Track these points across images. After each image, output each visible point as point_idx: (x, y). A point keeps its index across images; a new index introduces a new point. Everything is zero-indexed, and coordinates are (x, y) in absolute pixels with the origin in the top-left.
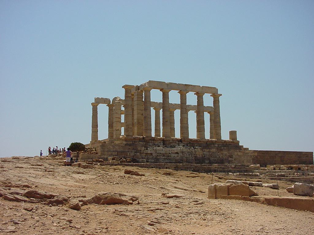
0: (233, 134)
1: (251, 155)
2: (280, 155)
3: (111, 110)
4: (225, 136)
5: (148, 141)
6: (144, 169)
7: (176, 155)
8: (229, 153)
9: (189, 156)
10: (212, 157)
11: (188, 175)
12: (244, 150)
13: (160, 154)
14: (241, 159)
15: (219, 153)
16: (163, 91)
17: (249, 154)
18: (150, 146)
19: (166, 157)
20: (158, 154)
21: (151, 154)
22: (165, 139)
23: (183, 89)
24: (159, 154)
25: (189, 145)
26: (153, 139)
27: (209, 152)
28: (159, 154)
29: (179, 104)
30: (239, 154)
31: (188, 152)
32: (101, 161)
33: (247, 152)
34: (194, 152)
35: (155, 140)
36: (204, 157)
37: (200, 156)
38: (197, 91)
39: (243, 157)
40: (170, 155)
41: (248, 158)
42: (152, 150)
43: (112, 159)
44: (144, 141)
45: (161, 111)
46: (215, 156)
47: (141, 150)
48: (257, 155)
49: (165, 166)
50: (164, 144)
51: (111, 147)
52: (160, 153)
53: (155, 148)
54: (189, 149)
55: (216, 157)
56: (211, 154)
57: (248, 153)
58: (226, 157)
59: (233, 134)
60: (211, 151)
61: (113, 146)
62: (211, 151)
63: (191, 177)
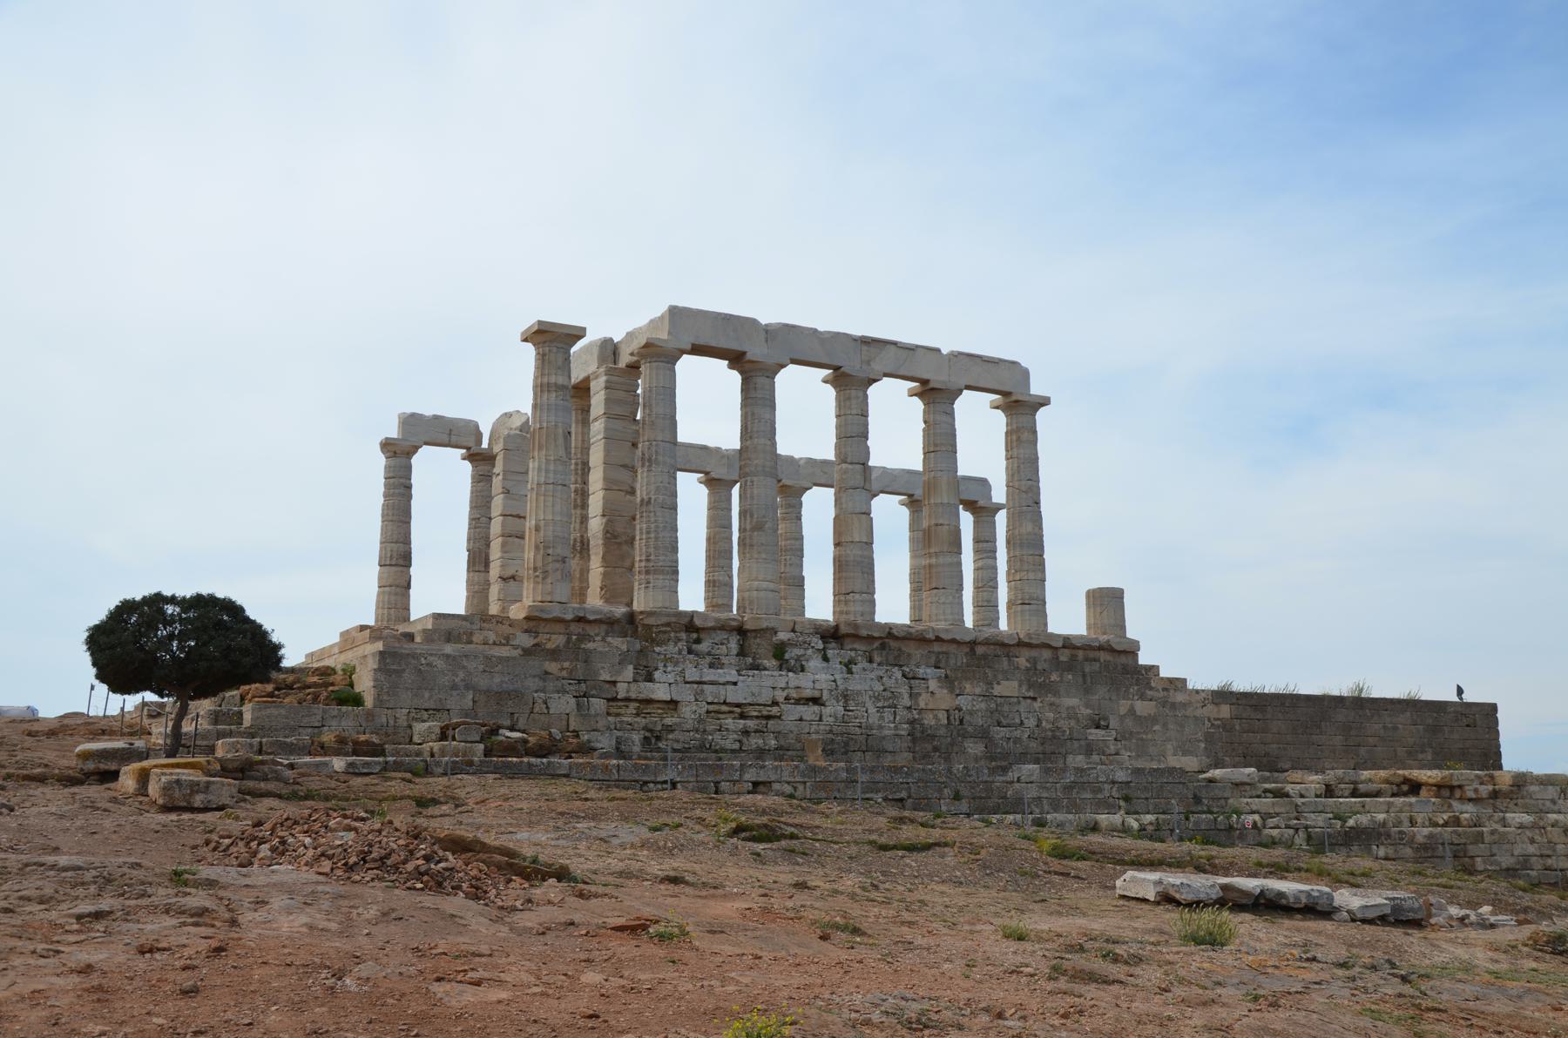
0: (1107, 602)
3: (482, 480)
4: (1067, 618)
5: (656, 634)
6: (613, 799)
7: (809, 711)
8: (1087, 706)
9: (882, 718)
10: (999, 724)
11: (883, 840)
12: (1165, 689)
15: (1037, 705)
16: (747, 366)
18: (666, 660)
19: (751, 724)
20: (711, 708)
21: (673, 704)
22: (747, 627)
23: (853, 366)
24: (715, 707)
25: (877, 659)
26: (685, 620)
27: (987, 696)
28: (715, 707)
29: (825, 462)
30: (1143, 708)
31: (877, 698)
32: (367, 742)
33: (1180, 698)
34: (906, 696)
35: (697, 630)
36: (961, 721)
37: (935, 717)
38: (925, 376)
39: (1156, 728)
40: (775, 710)
42: (676, 682)
43: (438, 731)
44: (635, 634)
45: (736, 491)
47: (614, 683)
49: (747, 777)
50: (742, 653)
51: (440, 664)
52: (725, 703)
53: (692, 674)
55: (1022, 723)
56: (993, 705)
57: (1184, 705)
58: (1073, 723)
59: (1107, 602)
60: (997, 690)
61: (448, 656)
62: (997, 690)
63: (900, 853)
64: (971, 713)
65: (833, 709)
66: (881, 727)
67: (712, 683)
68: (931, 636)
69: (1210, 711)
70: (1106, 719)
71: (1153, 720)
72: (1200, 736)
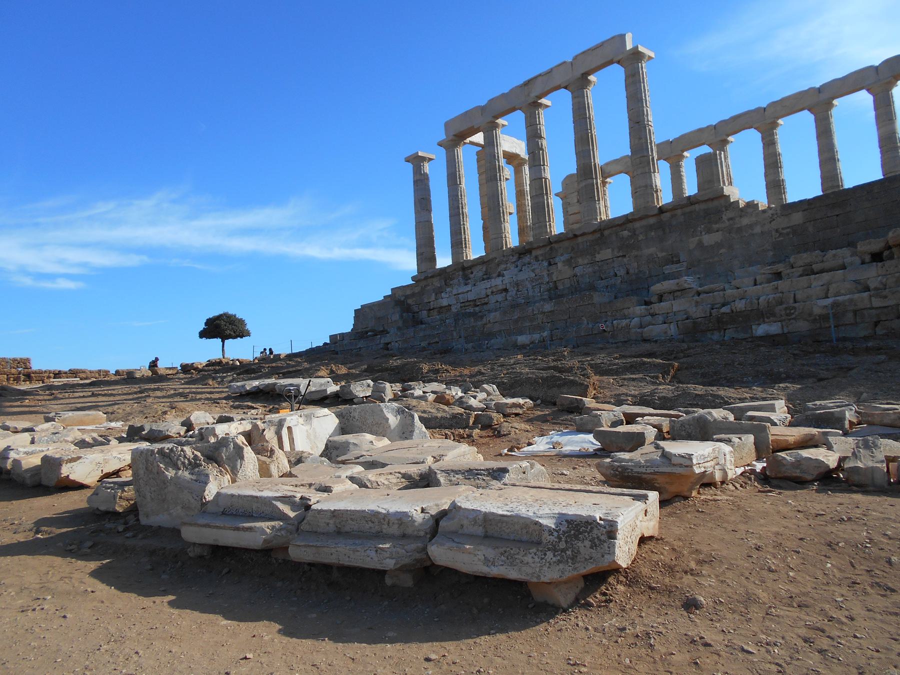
14: (716, 259)
15: (625, 260)
17: (758, 230)
19: (477, 309)
25: (540, 258)
27: (592, 263)
33: (745, 221)
34: (546, 276)
39: (722, 251)
46: (612, 274)
54: (533, 271)
55: (616, 275)
56: (597, 268)
57: (751, 226)
60: (598, 257)
62: (598, 257)
64: (582, 276)
65: (512, 292)
66: (534, 297)
71: (719, 245)
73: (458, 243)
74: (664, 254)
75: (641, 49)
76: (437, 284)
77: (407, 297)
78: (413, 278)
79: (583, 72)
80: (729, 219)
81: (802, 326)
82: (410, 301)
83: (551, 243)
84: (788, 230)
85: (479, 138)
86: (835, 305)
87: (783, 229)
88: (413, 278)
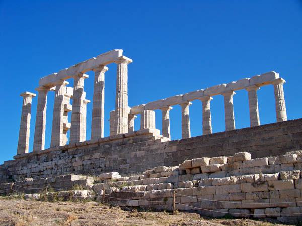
1: (162, 152)
2: (234, 140)
8: (120, 157)
13: (35, 174)
14: (141, 164)
17: (159, 152)
26: (36, 153)
27: (91, 159)
33: (155, 147)
39: (144, 160)
41: (156, 159)
48: (176, 150)
54: (65, 160)
55: (100, 167)
57: (156, 150)
60: (94, 157)
62: (94, 157)
64: (86, 165)
67: (34, 168)
68: (85, 144)
69: (168, 150)
70: (125, 160)
71: (143, 157)
72: (162, 161)
73: (37, 140)
74: (121, 159)
75: (124, 57)
76: (24, 161)
77: (9, 167)
78: (14, 157)
79: (101, 64)
80: (149, 145)
81: (146, 202)
82: (9, 169)
83: (77, 147)
84: (171, 154)
85: (54, 88)
86: (158, 194)
87: (169, 153)
88: (14, 157)
